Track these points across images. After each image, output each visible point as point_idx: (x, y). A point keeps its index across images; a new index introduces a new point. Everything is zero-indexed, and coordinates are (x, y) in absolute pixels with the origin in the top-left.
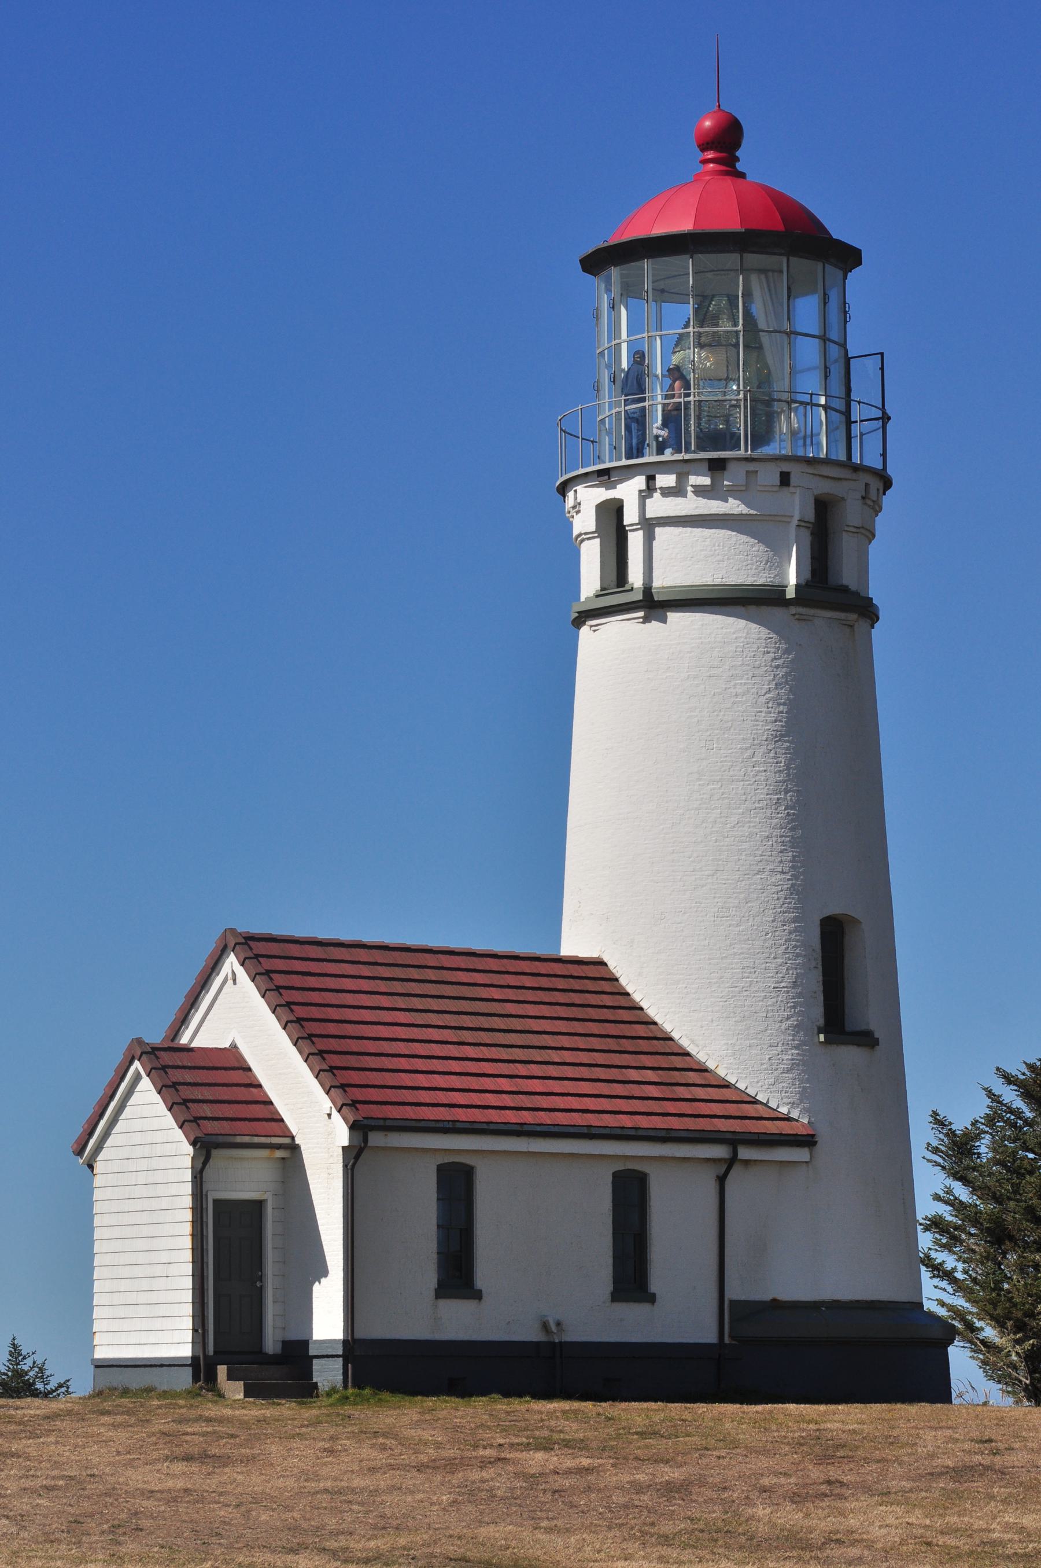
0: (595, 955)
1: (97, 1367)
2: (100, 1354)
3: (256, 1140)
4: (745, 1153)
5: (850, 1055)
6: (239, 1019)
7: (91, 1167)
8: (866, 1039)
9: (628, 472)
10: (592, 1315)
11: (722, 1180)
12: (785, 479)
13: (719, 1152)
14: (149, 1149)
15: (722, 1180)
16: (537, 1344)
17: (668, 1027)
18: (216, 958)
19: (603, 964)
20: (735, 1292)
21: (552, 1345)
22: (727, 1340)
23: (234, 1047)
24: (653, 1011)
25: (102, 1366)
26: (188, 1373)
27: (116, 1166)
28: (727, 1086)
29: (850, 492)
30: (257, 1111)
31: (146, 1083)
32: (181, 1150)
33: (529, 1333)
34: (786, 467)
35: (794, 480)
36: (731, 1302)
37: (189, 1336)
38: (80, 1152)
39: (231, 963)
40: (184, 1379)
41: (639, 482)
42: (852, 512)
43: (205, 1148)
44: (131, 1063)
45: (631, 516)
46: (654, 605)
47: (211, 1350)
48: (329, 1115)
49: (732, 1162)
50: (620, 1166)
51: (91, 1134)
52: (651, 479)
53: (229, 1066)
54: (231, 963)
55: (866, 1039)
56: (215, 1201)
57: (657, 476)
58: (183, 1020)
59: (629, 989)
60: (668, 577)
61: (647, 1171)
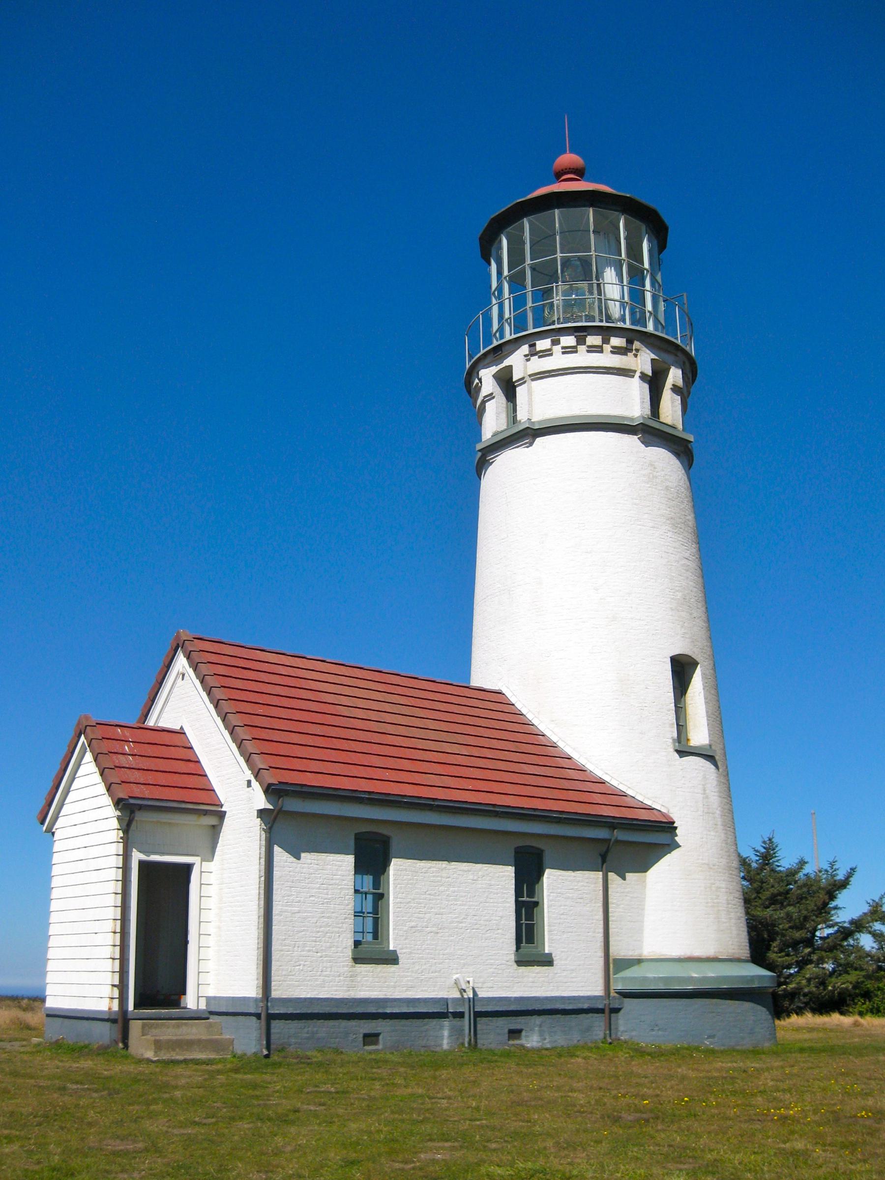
1: (48, 1016)
3: (183, 806)
6: (185, 706)
9: (516, 343)
13: (601, 833)
14: (88, 815)
18: (170, 657)
23: (181, 733)
31: (89, 757)
36: (615, 960)
38: (42, 823)
40: (104, 1033)
41: (525, 349)
43: (129, 810)
47: (131, 1007)
50: (521, 843)
51: (50, 805)
52: (533, 346)
53: (175, 746)
56: (141, 863)
57: (537, 342)
58: (146, 715)
61: (543, 848)
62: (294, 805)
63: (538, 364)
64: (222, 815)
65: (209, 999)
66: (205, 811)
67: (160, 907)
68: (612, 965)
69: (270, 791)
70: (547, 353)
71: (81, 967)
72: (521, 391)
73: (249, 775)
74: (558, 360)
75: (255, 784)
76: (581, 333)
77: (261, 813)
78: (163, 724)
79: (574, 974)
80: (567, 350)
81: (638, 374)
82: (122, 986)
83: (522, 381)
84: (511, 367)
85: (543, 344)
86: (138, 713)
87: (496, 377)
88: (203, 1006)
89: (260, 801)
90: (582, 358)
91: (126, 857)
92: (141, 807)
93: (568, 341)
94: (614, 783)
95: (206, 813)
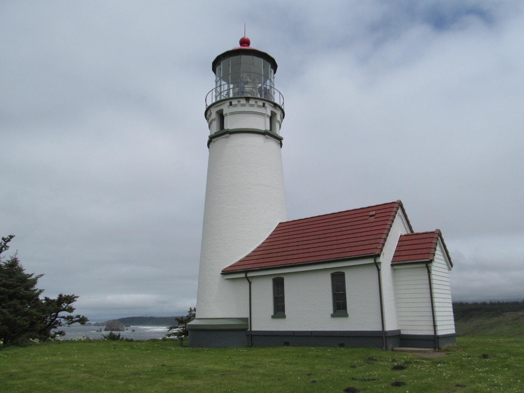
29: (278, 113)
34: (264, 102)
42: (278, 118)
70: (236, 106)
72: (225, 118)
74: (240, 109)
76: (248, 99)
80: (243, 105)
84: (222, 110)
85: (234, 102)
87: (217, 112)
90: (247, 109)
93: (243, 101)
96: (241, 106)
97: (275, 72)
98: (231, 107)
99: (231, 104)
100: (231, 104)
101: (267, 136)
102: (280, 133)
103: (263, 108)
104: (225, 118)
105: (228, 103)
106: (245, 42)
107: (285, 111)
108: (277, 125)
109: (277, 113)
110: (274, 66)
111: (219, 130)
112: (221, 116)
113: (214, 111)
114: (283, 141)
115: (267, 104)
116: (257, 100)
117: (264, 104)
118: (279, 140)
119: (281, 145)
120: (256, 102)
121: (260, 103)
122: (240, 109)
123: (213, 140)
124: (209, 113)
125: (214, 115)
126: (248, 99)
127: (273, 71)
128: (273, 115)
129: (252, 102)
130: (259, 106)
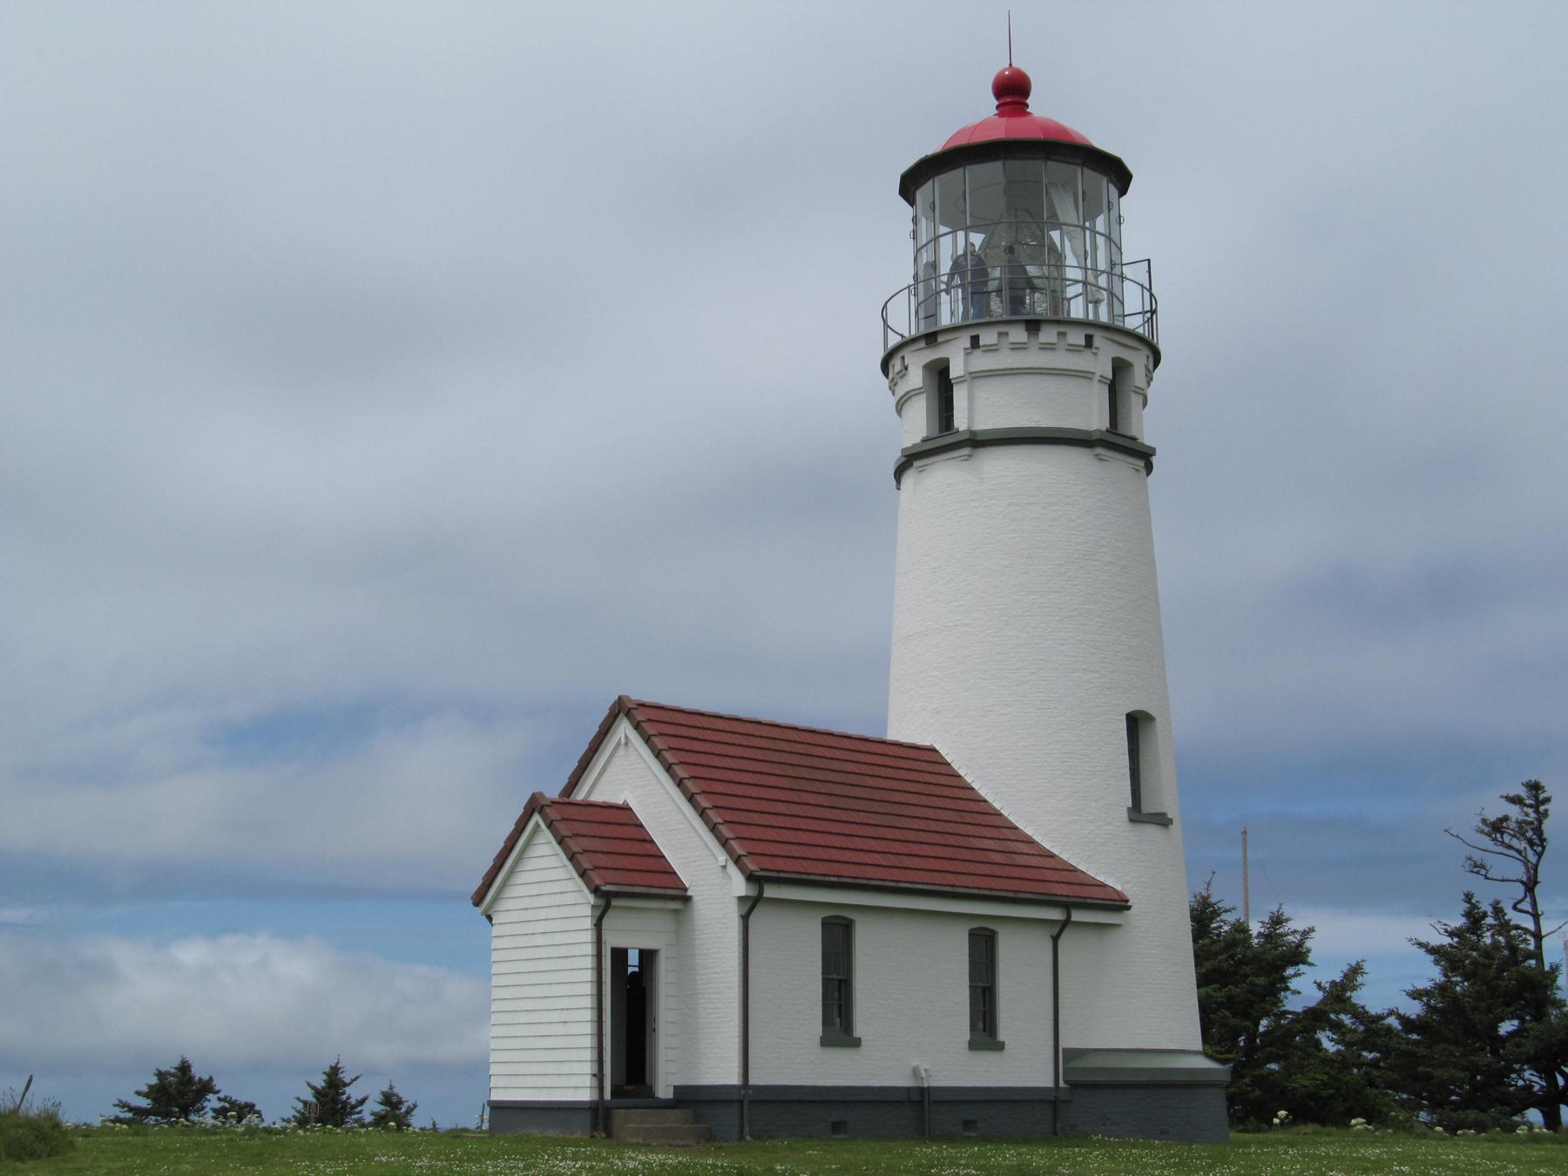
0: (927, 743)
2: (496, 1096)
3: (653, 891)
4: (1077, 916)
5: (1151, 831)
6: (634, 781)
7: (490, 918)
8: (1162, 821)
10: (954, 1066)
11: (1055, 939)
12: (1089, 341)
13: (1056, 915)
15: (1055, 939)
16: (909, 1089)
17: (997, 805)
19: (934, 750)
20: (1067, 1042)
21: (922, 1090)
22: (1062, 1084)
24: (983, 792)
25: (497, 1107)
26: (587, 1117)
27: (514, 916)
28: (1053, 856)
29: (1139, 360)
30: (651, 864)
31: (546, 835)
32: (581, 902)
33: (902, 1080)
34: (1090, 331)
35: (1097, 341)
37: (588, 1081)
39: (624, 729)
43: (605, 901)
44: (531, 815)
45: (955, 371)
46: (978, 442)
47: (608, 1096)
48: (724, 867)
49: (1066, 924)
54: (624, 729)
55: (1162, 821)
59: (961, 772)
60: (987, 421)
62: (771, 892)
63: (981, 362)
64: (687, 899)
65: (677, 1089)
66: (669, 892)
67: (630, 997)
68: (1065, 1058)
69: (750, 878)
70: (992, 349)
71: (553, 1055)
73: (722, 857)
74: (1005, 360)
75: (733, 870)
76: (1033, 326)
77: (741, 899)
78: (597, 798)
79: (1024, 1064)
80: (1018, 347)
81: (1097, 377)
82: (599, 1076)
83: (961, 380)
84: (947, 360)
85: (988, 337)
86: (563, 782)
88: (670, 1095)
89: (739, 885)
91: (599, 942)
92: (617, 895)
93: (1018, 334)
94: (1064, 856)
95: (673, 898)
96: (1008, 349)
97: (1123, 191)
98: (977, 353)
99: (975, 341)
100: (975, 341)
101: (1099, 450)
102: (1147, 426)
103: (1087, 353)
104: (955, 388)
105: (965, 341)
106: (1012, 91)
107: (1162, 347)
108: (1136, 400)
109: (1131, 354)
110: (1119, 175)
111: (936, 434)
112: (941, 381)
113: (916, 364)
114: (1154, 460)
115: (1098, 341)
116: (1062, 329)
117: (1089, 341)
118: (1144, 456)
119: (1149, 468)
120: (1062, 335)
121: (1077, 337)
122: (1005, 360)
123: (916, 464)
124: (896, 365)
125: (916, 378)
126: (1033, 326)
127: (1114, 191)
128: (1120, 367)
129: (1048, 335)
130: (1073, 349)
